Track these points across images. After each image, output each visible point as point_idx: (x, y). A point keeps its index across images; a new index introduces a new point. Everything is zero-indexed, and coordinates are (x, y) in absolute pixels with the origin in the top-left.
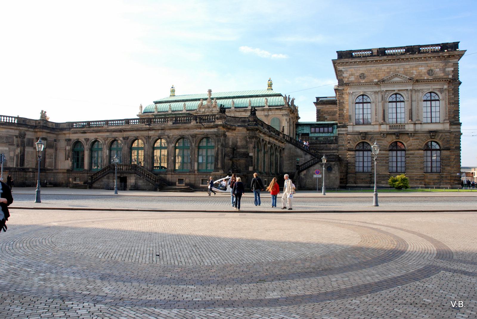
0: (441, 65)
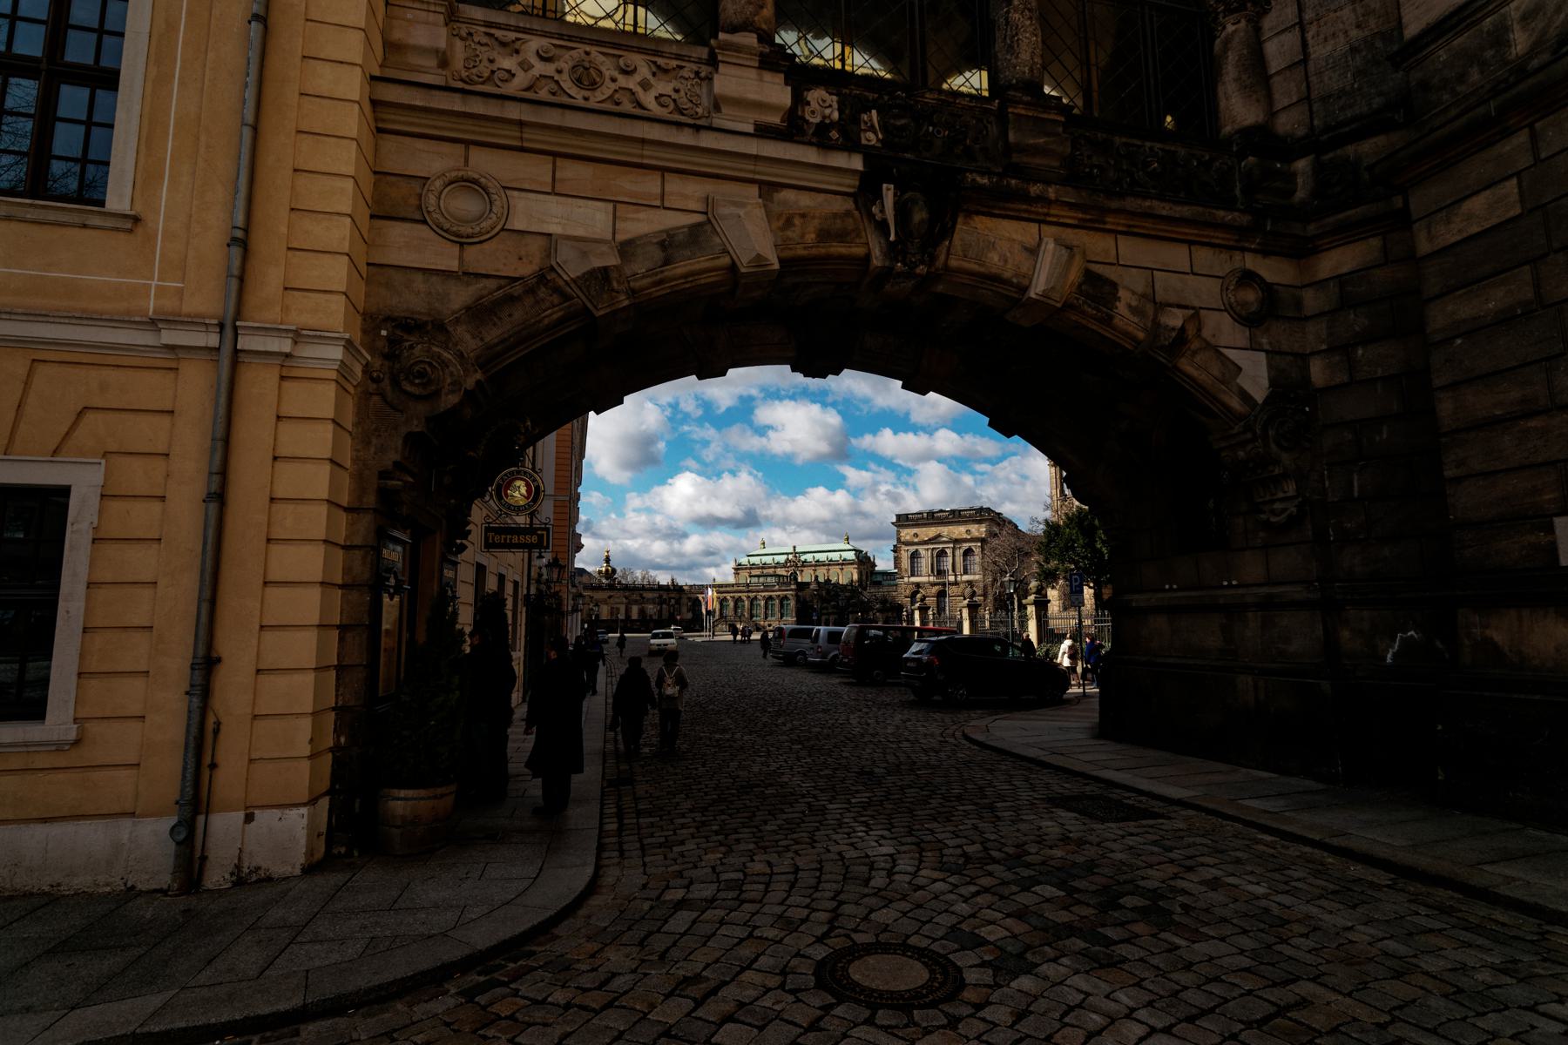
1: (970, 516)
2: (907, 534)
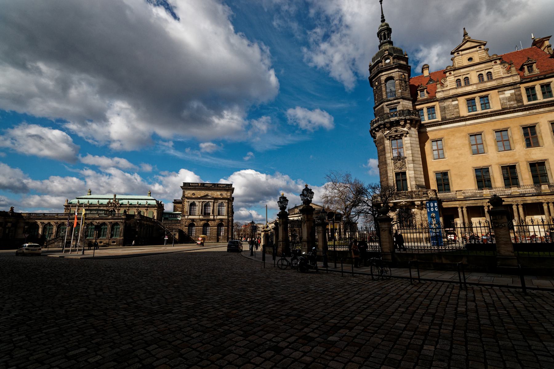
1: (223, 187)
2: (189, 193)
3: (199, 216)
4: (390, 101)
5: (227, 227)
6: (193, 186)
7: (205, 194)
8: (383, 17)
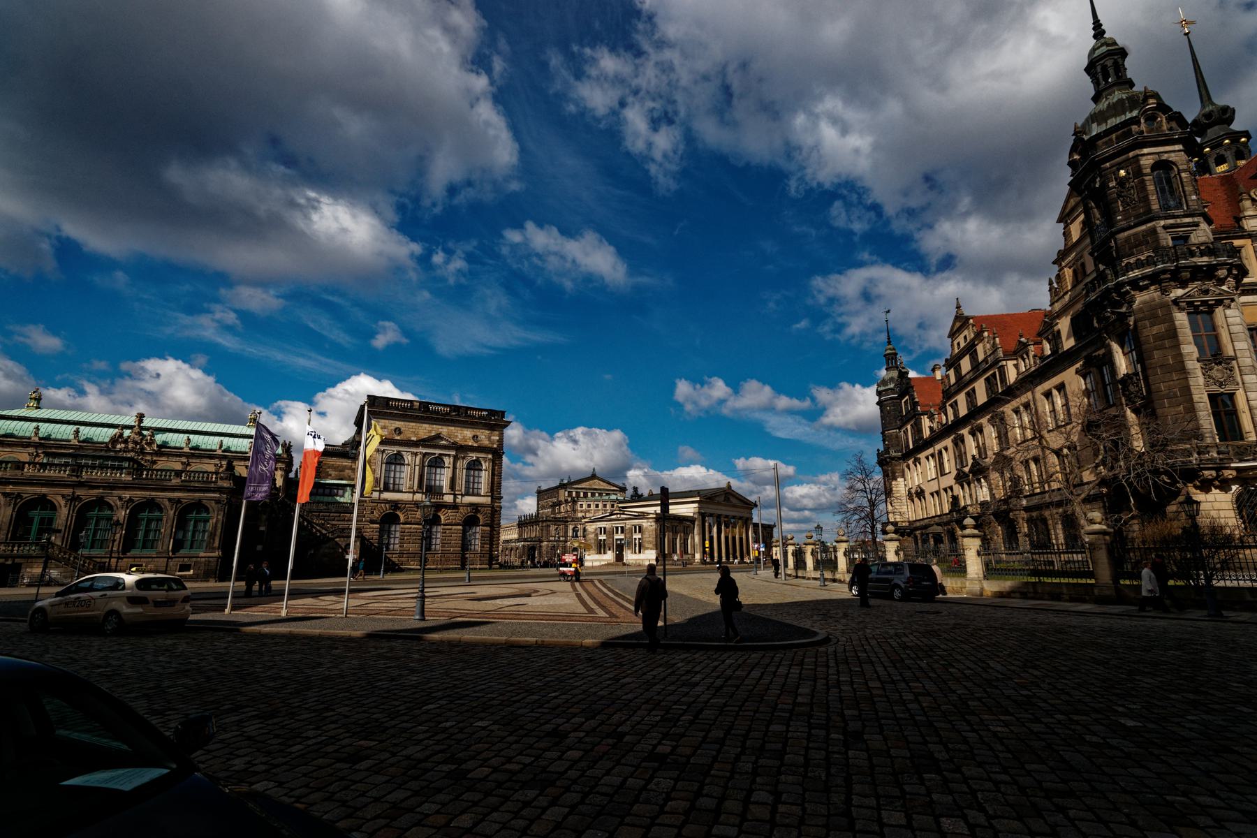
0: (487, 432)
1: (480, 417)
3: (414, 493)
4: (1174, 217)
5: (488, 528)
6: (396, 408)
7: (430, 432)
8: (1097, 25)
